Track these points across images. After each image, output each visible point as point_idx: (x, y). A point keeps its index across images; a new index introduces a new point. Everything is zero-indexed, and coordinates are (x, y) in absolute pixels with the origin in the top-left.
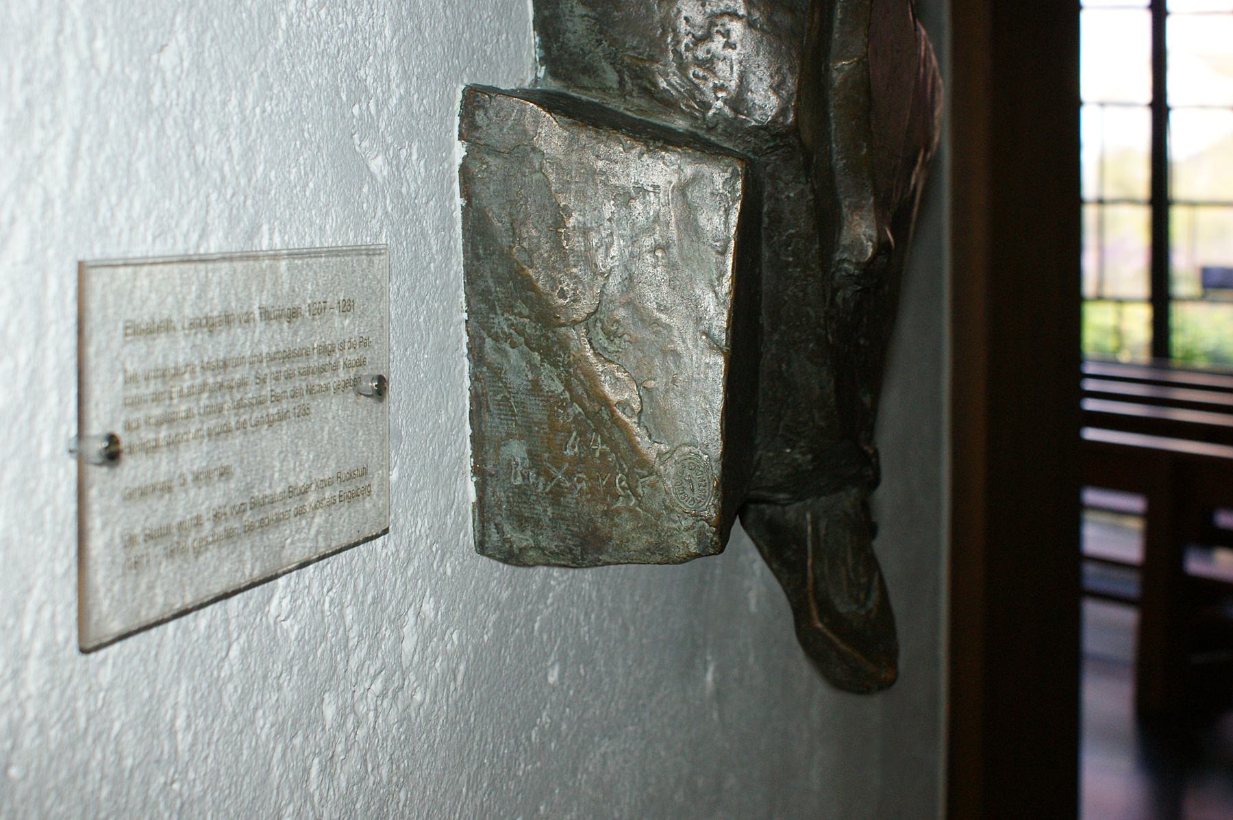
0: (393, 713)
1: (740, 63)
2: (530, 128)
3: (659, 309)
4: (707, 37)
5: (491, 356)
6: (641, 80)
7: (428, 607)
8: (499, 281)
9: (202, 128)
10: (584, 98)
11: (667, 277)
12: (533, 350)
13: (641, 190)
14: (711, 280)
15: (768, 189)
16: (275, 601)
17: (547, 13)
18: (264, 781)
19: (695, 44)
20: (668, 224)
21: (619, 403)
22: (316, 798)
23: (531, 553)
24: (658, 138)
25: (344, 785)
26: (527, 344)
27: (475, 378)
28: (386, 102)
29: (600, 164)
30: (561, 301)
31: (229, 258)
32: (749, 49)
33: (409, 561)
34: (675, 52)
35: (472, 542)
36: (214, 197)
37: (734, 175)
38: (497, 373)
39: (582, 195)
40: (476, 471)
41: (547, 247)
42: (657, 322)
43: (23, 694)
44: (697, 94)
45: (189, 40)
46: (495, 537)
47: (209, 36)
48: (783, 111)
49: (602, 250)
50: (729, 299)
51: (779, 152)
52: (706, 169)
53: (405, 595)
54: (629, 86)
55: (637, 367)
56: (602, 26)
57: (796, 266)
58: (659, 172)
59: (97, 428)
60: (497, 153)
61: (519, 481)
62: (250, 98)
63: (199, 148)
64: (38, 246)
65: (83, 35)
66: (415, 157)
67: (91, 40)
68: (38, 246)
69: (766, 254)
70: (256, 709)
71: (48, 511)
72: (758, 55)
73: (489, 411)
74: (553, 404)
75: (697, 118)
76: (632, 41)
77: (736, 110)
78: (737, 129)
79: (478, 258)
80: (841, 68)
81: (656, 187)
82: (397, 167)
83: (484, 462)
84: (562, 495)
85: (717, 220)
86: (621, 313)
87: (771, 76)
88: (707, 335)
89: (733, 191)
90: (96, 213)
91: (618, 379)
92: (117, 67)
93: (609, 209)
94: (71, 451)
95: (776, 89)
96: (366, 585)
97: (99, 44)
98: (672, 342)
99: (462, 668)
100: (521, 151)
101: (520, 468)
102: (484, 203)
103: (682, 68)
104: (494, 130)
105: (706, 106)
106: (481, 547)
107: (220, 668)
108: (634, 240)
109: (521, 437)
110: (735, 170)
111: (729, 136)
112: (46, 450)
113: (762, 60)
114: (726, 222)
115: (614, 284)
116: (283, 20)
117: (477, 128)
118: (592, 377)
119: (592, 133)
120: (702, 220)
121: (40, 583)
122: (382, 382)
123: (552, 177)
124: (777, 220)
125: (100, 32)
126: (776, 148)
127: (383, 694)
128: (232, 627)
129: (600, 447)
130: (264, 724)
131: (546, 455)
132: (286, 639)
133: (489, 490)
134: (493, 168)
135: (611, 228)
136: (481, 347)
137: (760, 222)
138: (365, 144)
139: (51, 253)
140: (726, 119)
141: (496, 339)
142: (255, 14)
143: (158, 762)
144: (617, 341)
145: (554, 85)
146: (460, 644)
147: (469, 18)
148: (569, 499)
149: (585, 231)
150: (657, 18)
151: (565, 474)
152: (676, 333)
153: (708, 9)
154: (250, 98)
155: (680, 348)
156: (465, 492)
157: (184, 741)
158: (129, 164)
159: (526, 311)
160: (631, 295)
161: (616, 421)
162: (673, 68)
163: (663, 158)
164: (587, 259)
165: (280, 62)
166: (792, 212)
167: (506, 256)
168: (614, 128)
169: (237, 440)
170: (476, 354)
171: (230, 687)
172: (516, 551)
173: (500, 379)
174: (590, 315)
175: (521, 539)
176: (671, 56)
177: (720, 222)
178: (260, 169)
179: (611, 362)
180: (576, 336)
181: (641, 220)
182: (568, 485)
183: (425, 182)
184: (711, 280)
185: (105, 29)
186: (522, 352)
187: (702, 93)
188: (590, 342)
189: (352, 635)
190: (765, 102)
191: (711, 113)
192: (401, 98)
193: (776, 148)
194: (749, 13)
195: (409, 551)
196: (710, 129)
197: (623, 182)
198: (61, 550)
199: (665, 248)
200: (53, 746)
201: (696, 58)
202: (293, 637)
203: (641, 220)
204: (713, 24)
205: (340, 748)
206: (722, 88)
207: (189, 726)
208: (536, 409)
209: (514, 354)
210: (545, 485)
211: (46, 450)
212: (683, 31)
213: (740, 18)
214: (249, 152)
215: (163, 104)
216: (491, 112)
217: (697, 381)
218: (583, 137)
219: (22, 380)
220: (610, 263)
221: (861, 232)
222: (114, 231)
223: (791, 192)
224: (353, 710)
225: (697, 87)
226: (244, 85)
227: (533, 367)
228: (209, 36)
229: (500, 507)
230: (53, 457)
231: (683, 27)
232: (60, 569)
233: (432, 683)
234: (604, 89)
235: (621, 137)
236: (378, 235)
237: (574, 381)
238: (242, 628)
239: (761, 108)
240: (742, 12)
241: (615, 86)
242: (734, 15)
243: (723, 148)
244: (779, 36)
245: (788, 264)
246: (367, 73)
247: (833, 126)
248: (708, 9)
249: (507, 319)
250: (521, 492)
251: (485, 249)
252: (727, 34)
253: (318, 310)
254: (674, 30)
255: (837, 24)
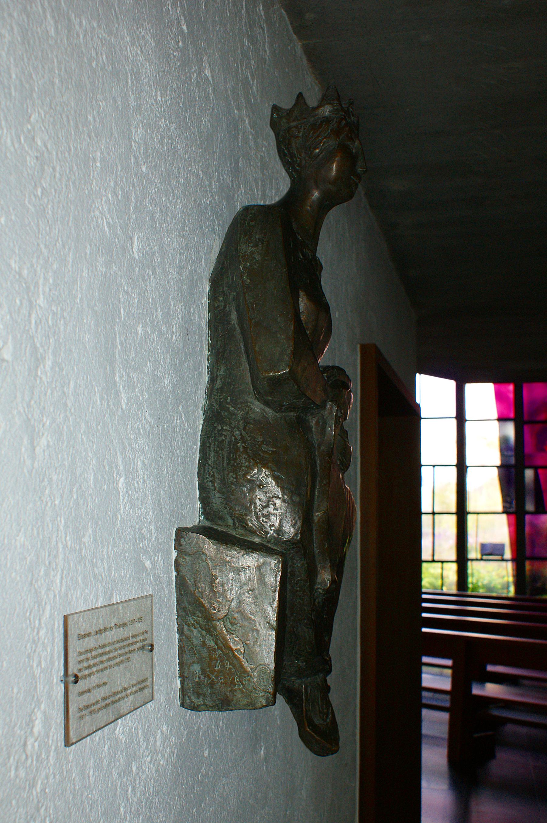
0: (154, 769)
1: (280, 516)
2: (201, 545)
3: (251, 614)
4: (267, 506)
5: (186, 632)
6: (242, 522)
7: (165, 729)
8: (190, 604)
9: (96, 561)
10: (219, 529)
11: (254, 601)
12: (203, 630)
13: (243, 568)
14: (270, 603)
15: (290, 563)
16: (118, 729)
17: (204, 495)
18: (115, 794)
19: (263, 509)
20: (254, 581)
21: (236, 649)
22: (130, 800)
23: (202, 707)
24: (250, 547)
25: (139, 795)
26: (200, 627)
27: (180, 640)
28: (151, 540)
29: (228, 558)
30: (214, 611)
31: (105, 606)
32: (283, 511)
33: (159, 711)
34: (255, 512)
35: (179, 703)
36: (100, 586)
37: (279, 562)
38: (189, 638)
39: (221, 571)
40: (180, 676)
41: (208, 591)
42: (250, 618)
43: (49, 765)
44: (263, 528)
45: (92, 531)
46: (188, 701)
47: (98, 528)
48: (296, 534)
49: (229, 591)
50: (277, 609)
51: (295, 550)
52: (268, 559)
53: (157, 725)
54: (237, 525)
55: (243, 636)
56: (227, 501)
57: (300, 591)
58: (250, 561)
59: (70, 672)
60: (189, 555)
61: (197, 679)
62: (110, 548)
63: (95, 569)
64: (53, 612)
65: (64, 536)
66: (160, 559)
67: (66, 537)
68: (53, 612)
69: (289, 587)
70: (113, 768)
71: (55, 702)
72: (286, 512)
73: (185, 653)
74: (211, 650)
75: (263, 538)
76: (238, 508)
77: (278, 534)
78: (279, 542)
79: (181, 595)
80: (318, 515)
81: (249, 567)
82: (154, 563)
83: (183, 672)
84: (214, 684)
85: (272, 579)
86: (236, 615)
87: (292, 521)
88: (269, 623)
89: (279, 568)
90: (68, 597)
91: (235, 640)
92: (73, 545)
93: (231, 576)
94: (62, 681)
95: (293, 526)
96: (145, 721)
97: (68, 538)
98: (256, 626)
99: (176, 751)
100: (198, 554)
101: (198, 675)
102: (184, 574)
103: (258, 518)
104: (188, 546)
105: (267, 533)
106: (183, 705)
107: (102, 754)
108: (241, 587)
109: (199, 663)
110: (279, 560)
111: (275, 544)
112: (55, 680)
113: (288, 515)
114: (276, 580)
115: (234, 604)
116: (119, 517)
117: (181, 545)
118: (226, 640)
119: (225, 547)
120: (267, 579)
121: (53, 726)
122: (152, 646)
123: (210, 564)
124: (293, 574)
125: (68, 534)
126: (293, 548)
127: (151, 762)
128: (106, 739)
129: (229, 666)
130: (115, 775)
131: (208, 670)
132: (121, 742)
133: (186, 683)
134: (187, 561)
135: (232, 583)
136: (183, 628)
137: (287, 576)
138: (144, 557)
139: (56, 613)
140: (275, 538)
141: (188, 626)
142: (111, 517)
143: (85, 787)
144: (235, 626)
145: (207, 523)
146: (175, 742)
147: (177, 502)
148: (217, 686)
149: (223, 584)
150: (248, 499)
151: (215, 677)
152: (257, 622)
153: (268, 495)
154: (110, 548)
155: (259, 628)
156: (176, 684)
157: (92, 780)
158: (76, 579)
159: (200, 615)
160: (240, 608)
161: (235, 656)
162: (254, 518)
163: (252, 556)
164: (223, 595)
165: (119, 533)
166: (299, 571)
167: (193, 594)
168: (234, 545)
169: (107, 672)
170: (181, 631)
171: (105, 760)
172: (196, 706)
173: (190, 641)
174: (225, 616)
175: (198, 702)
176: (253, 513)
177: (273, 579)
178: (113, 573)
179: (233, 634)
180: (220, 625)
181: (244, 580)
182: (216, 681)
183: (163, 568)
184: (270, 603)
185: (70, 533)
186: (198, 631)
187: (265, 528)
188: (225, 627)
189: (141, 740)
190: (289, 530)
191: (269, 535)
192: (156, 538)
193: (293, 548)
194: (283, 497)
195: (158, 708)
196: (268, 542)
197: (237, 565)
198: (59, 715)
199: (253, 591)
200: (57, 782)
201: (263, 514)
202: (123, 742)
203: (244, 580)
204: (269, 501)
205: (137, 782)
206: (273, 526)
207: (94, 775)
208: (204, 653)
209: (195, 631)
210: (207, 681)
211: (55, 680)
212: (258, 504)
213: (280, 498)
214: (110, 567)
215: (85, 555)
216: (187, 540)
217: (265, 641)
218: (222, 548)
219: (49, 658)
220: (232, 597)
221: (325, 577)
222: (72, 603)
223: (299, 564)
224: (142, 768)
225: (263, 525)
226: (108, 543)
227: (203, 636)
228: (98, 528)
229: (190, 690)
230: (57, 683)
231: (258, 502)
232: (59, 721)
233: (166, 756)
234: (228, 526)
235: (236, 548)
236: (148, 591)
237: (219, 642)
238: (108, 739)
239: (288, 533)
240: (280, 496)
241: (232, 525)
242: (277, 497)
243: (274, 550)
244: (294, 505)
245: (297, 591)
246: (145, 531)
247: (315, 537)
248: (268, 495)
249: (193, 618)
250: (198, 684)
251: (185, 592)
252: (275, 505)
253: (132, 622)
254: (254, 504)
255: (316, 497)
